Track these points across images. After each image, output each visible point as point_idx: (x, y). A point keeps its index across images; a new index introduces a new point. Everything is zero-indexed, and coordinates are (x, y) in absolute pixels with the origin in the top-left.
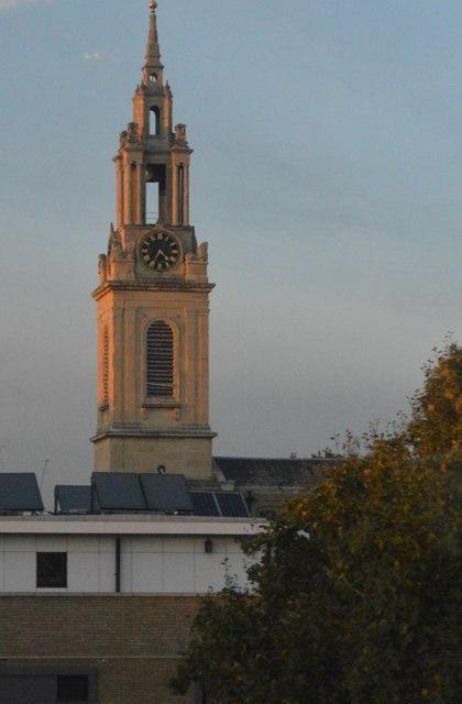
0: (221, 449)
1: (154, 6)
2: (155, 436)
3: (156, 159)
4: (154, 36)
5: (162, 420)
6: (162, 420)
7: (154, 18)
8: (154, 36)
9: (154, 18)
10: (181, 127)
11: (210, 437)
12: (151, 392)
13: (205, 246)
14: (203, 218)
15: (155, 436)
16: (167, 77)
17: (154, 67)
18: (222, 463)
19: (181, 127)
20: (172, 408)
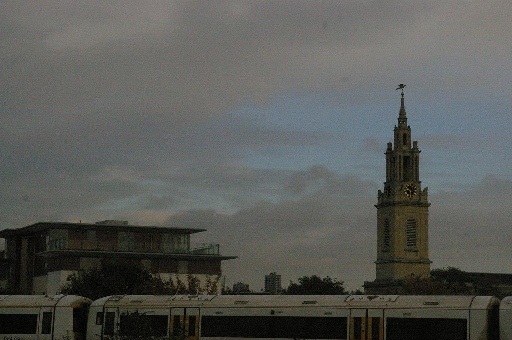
0: (434, 267)
1: (403, 95)
2: (411, 262)
3: (408, 154)
4: (403, 106)
5: (412, 256)
6: (412, 256)
7: (403, 99)
8: (403, 106)
9: (403, 99)
10: (416, 143)
11: (430, 263)
12: (408, 245)
13: (426, 189)
14: (430, 176)
15: (411, 262)
16: (409, 122)
17: (403, 118)
18: (434, 273)
19: (416, 143)
20: (417, 251)
